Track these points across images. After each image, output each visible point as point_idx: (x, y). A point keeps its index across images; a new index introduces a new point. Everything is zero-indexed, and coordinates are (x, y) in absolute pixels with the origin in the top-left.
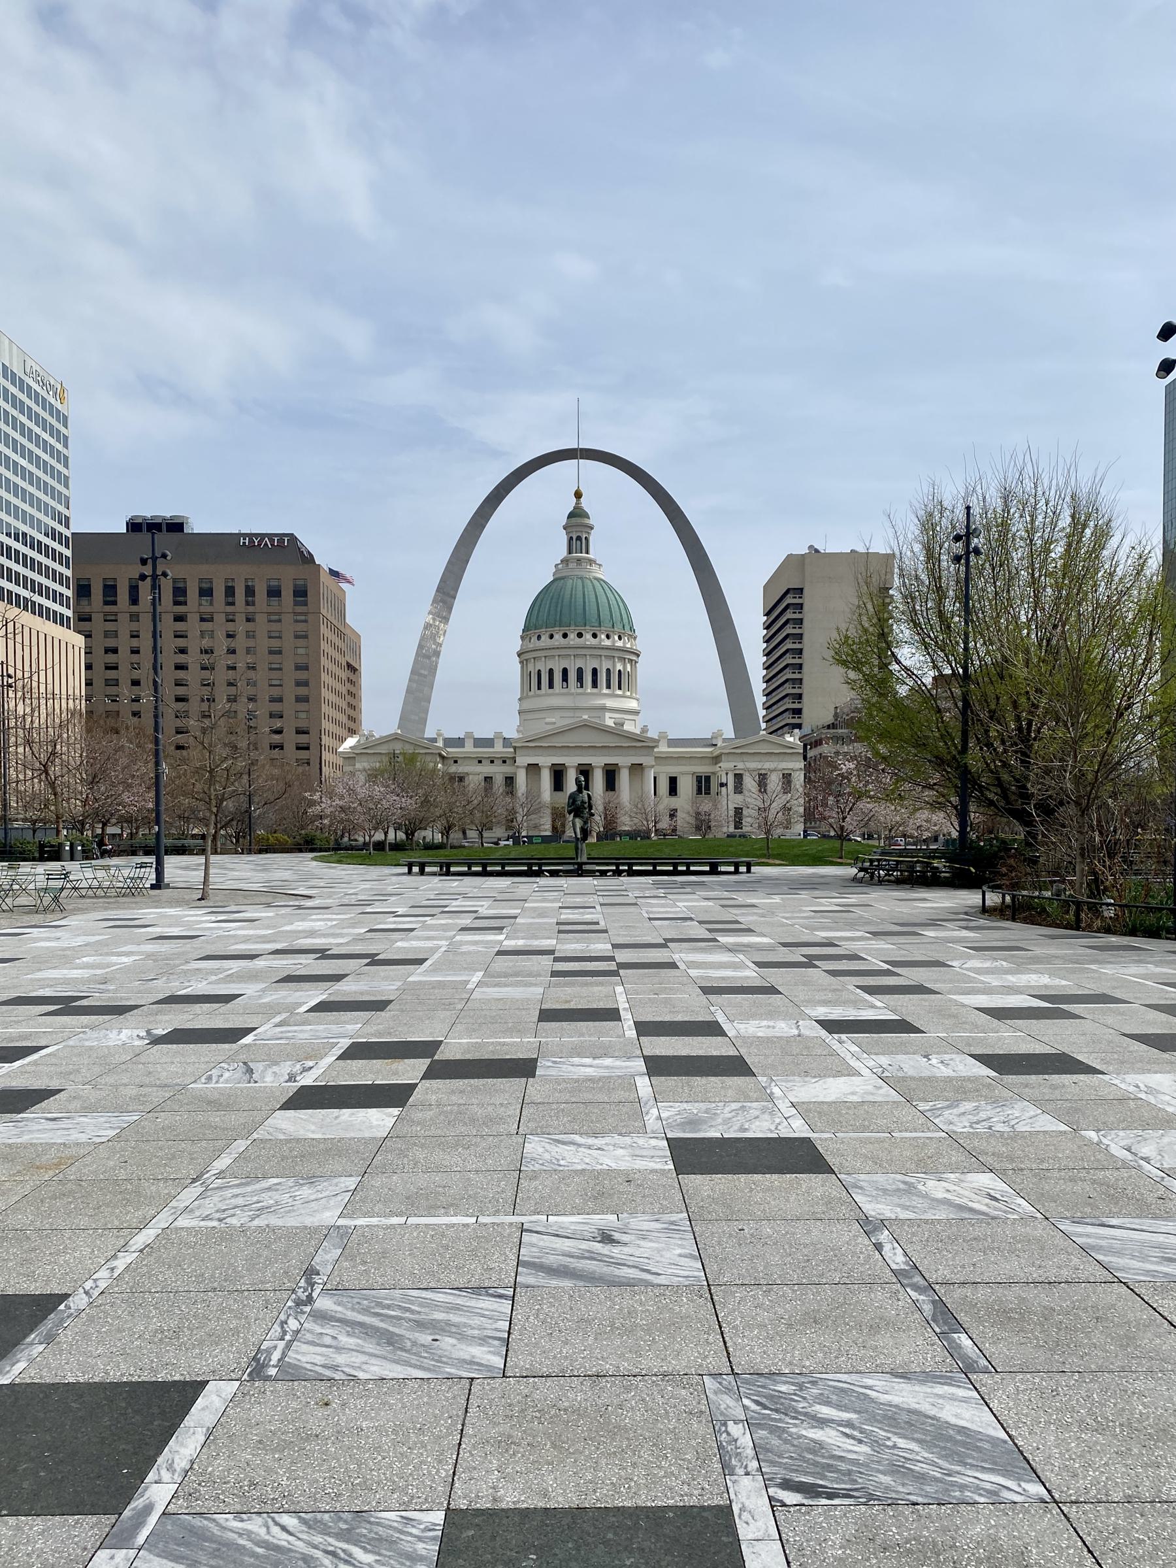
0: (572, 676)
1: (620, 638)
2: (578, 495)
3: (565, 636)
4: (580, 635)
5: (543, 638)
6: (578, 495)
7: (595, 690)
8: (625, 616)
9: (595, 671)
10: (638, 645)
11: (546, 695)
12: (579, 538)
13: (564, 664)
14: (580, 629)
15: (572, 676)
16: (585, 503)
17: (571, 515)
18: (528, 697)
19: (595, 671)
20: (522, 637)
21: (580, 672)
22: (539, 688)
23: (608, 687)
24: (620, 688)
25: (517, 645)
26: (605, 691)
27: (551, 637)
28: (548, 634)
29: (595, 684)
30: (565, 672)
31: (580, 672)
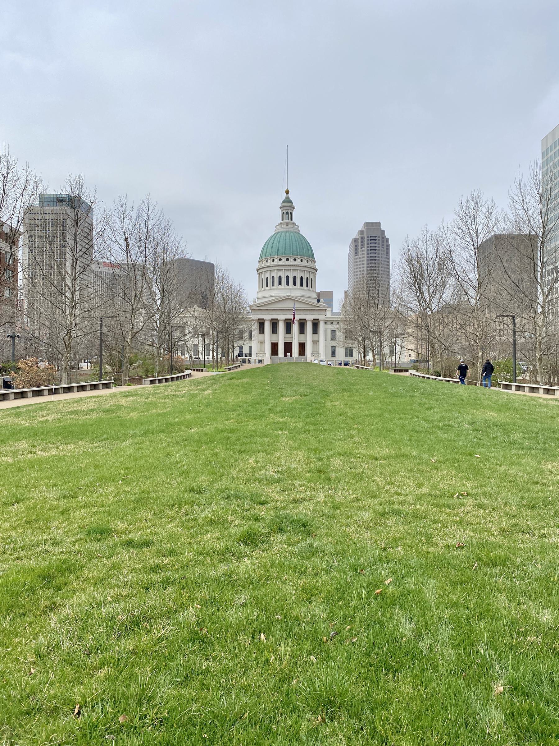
0: (283, 281)
1: (308, 261)
3: (280, 260)
4: (288, 260)
5: (269, 261)
6: (287, 192)
7: (295, 287)
9: (295, 278)
11: (271, 289)
12: (287, 213)
13: (280, 274)
14: (287, 256)
15: (283, 281)
17: (283, 202)
18: (262, 291)
19: (295, 278)
20: (259, 262)
21: (287, 278)
22: (267, 286)
23: (302, 285)
24: (307, 286)
25: (257, 266)
27: (273, 260)
29: (295, 284)
30: (280, 278)
31: (287, 278)
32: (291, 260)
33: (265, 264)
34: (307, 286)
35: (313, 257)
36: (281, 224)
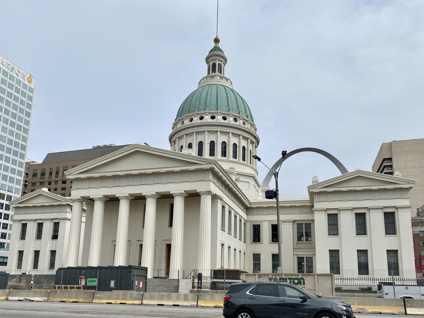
1: (244, 124)
2: (217, 41)
3: (202, 118)
6: (217, 41)
8: (248, 110)
9: (224, 144)
10: (258, 133)
13: (200, 138)
16: (220, 45)
21: (212, 144)
23: (235, 156)
24: (244, 159)
26: (231, 158)
27: (191, 120)
28: (189, 118)
29: (224, 154)
31: (212, 144)
32: (219, 119)
33: (179, 126)
34: (244, 159)
35: (253, 121)
36: (206, 77)
